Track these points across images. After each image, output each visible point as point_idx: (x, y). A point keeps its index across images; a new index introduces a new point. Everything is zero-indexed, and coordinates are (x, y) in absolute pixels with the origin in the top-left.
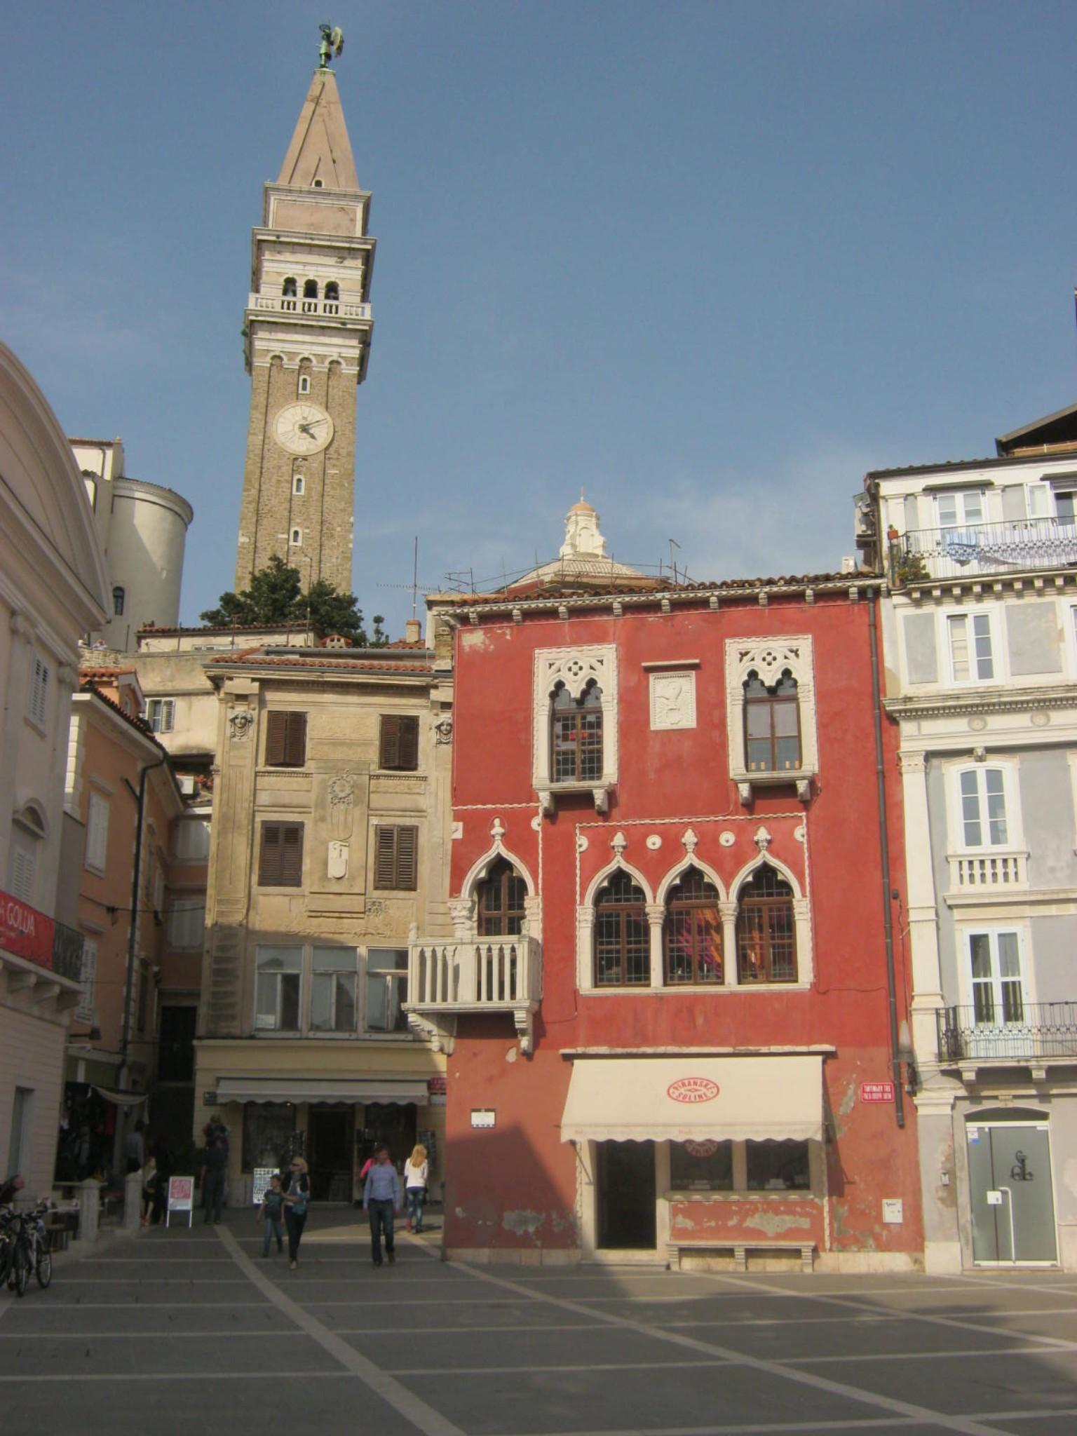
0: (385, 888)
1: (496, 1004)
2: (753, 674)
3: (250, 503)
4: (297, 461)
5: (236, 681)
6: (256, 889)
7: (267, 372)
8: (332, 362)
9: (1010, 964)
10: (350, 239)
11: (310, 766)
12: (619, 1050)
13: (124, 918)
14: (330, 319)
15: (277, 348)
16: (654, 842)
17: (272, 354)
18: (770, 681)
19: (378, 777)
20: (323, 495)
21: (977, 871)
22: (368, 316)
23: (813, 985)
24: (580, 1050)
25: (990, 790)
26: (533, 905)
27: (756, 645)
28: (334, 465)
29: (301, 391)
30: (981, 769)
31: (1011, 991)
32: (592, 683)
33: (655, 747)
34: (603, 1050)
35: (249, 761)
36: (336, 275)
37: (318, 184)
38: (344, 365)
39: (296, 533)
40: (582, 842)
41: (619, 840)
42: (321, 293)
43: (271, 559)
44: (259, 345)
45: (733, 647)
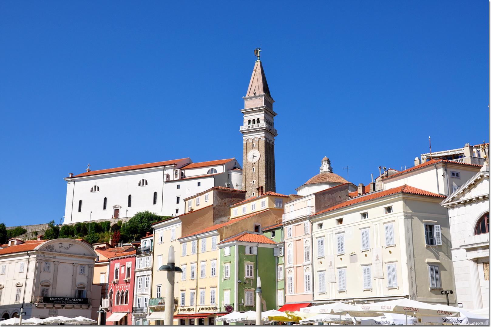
3: (244, 176)
7: (246, 144)
8: (259, 138)
10: (259, 108)
14: (257, 129)
16: (121, 287)
20: (259, 171)
22: (265, 126)
28: (261, 163)
29: (253, 147)
30: (141, 278)
36: (259, 116)
37: (255, 93)
38: (262, 139)
39: (254, 181)
40: (116, 287)
41: (118, 287)
42: (256, 122)
44: (244, 138)
45: (127, 263)
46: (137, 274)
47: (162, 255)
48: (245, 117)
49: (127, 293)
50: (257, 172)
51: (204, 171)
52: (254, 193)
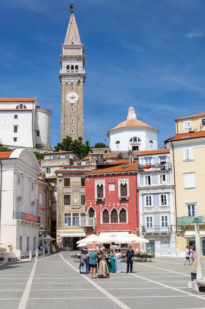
0: (83, 204)
1: (91, 226)
2: (122, 184)
3: (63, 114)
4: (72, 104)
5: (59, 174)
6: (64, 205)
9: (151, 221)
10: (80, 56)
11: (71, 186)
12: (106, 231)
13: (45, 210)
14: (77, 74)
15: (66, 81)
16: (110, 205)
17: (65, 82)
18: (124, 184)
19: (81, 188)
21: (148, 209)
22: (84, 73)
23: (128, 223)
24: (101, 231)
25: (150, 199)
26: (95, 213)
27: (122, 180)
29: (72, 90)
31: (151, 224)
32: (102, 185)
33: (110, 193)
34: (104, 231)
35: (62, 186)
37: (73, 43)
39: (72, 120)
42: (75, 68)
43: (66, 136)
44: (62, 80)
46: (141, 192)
47: (194, 173)
48: (64, 62)
49: (123, 211)
50: (76, 112)
51: (13, 106)
52: (72, 130)
